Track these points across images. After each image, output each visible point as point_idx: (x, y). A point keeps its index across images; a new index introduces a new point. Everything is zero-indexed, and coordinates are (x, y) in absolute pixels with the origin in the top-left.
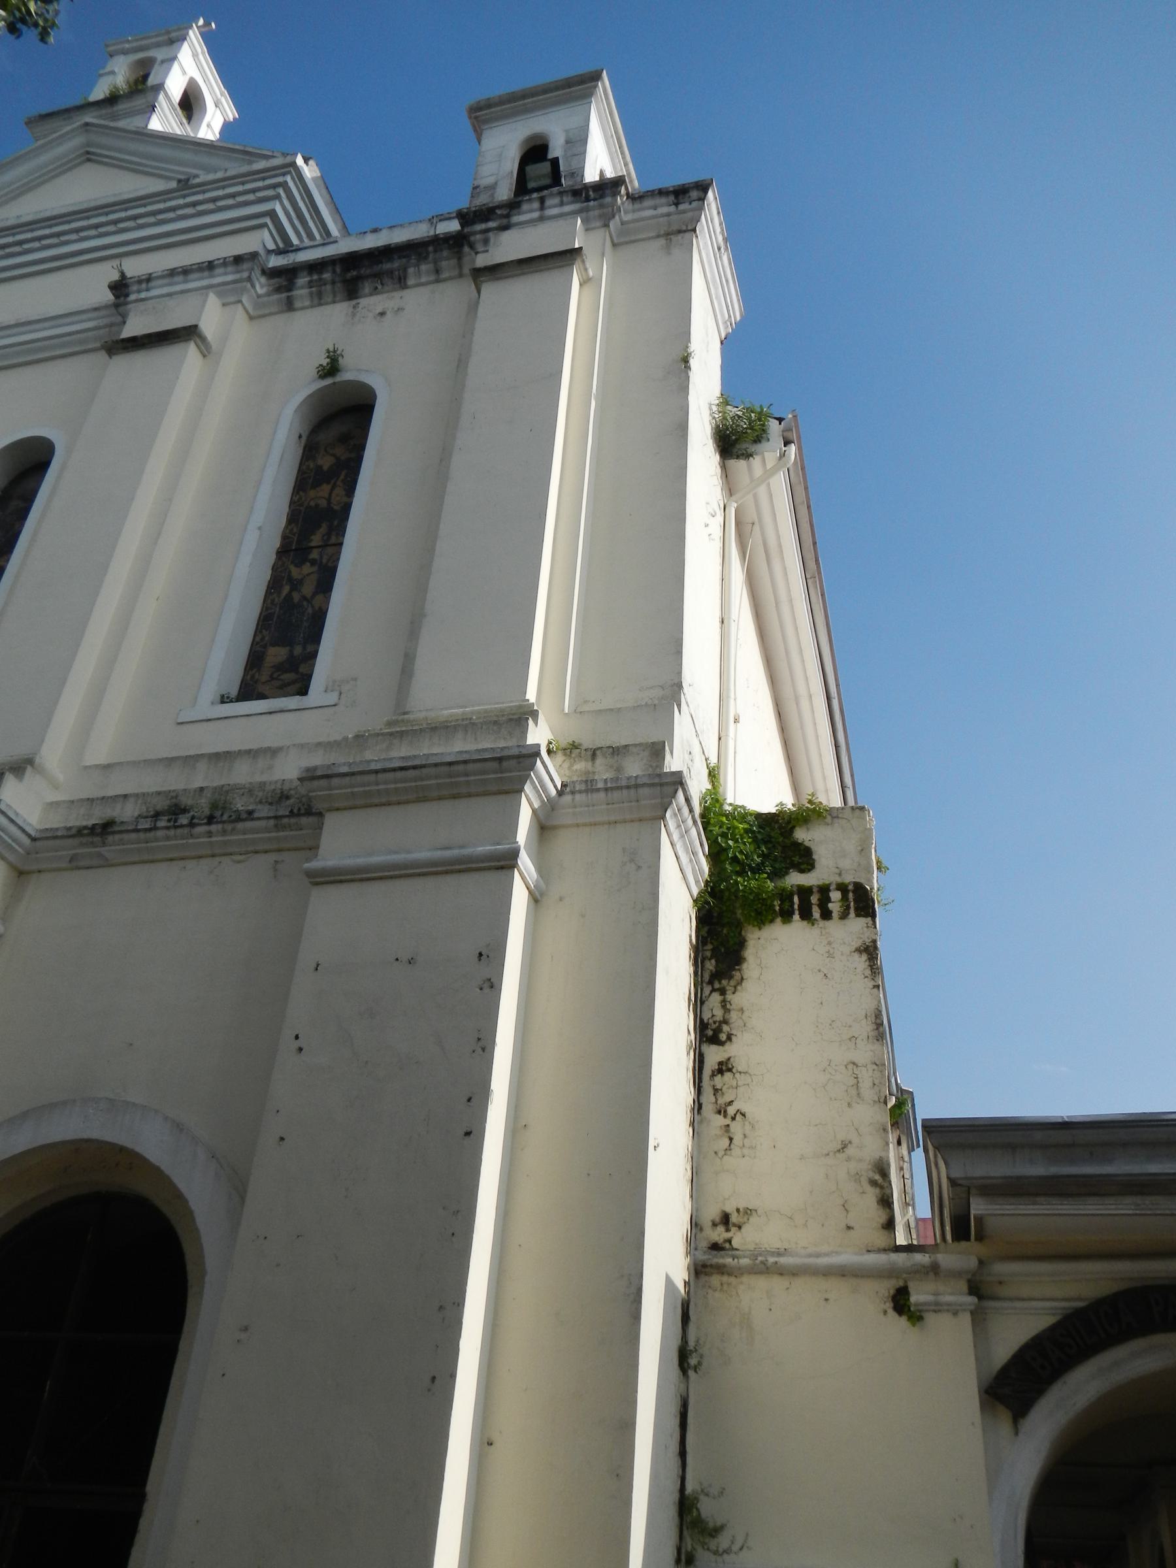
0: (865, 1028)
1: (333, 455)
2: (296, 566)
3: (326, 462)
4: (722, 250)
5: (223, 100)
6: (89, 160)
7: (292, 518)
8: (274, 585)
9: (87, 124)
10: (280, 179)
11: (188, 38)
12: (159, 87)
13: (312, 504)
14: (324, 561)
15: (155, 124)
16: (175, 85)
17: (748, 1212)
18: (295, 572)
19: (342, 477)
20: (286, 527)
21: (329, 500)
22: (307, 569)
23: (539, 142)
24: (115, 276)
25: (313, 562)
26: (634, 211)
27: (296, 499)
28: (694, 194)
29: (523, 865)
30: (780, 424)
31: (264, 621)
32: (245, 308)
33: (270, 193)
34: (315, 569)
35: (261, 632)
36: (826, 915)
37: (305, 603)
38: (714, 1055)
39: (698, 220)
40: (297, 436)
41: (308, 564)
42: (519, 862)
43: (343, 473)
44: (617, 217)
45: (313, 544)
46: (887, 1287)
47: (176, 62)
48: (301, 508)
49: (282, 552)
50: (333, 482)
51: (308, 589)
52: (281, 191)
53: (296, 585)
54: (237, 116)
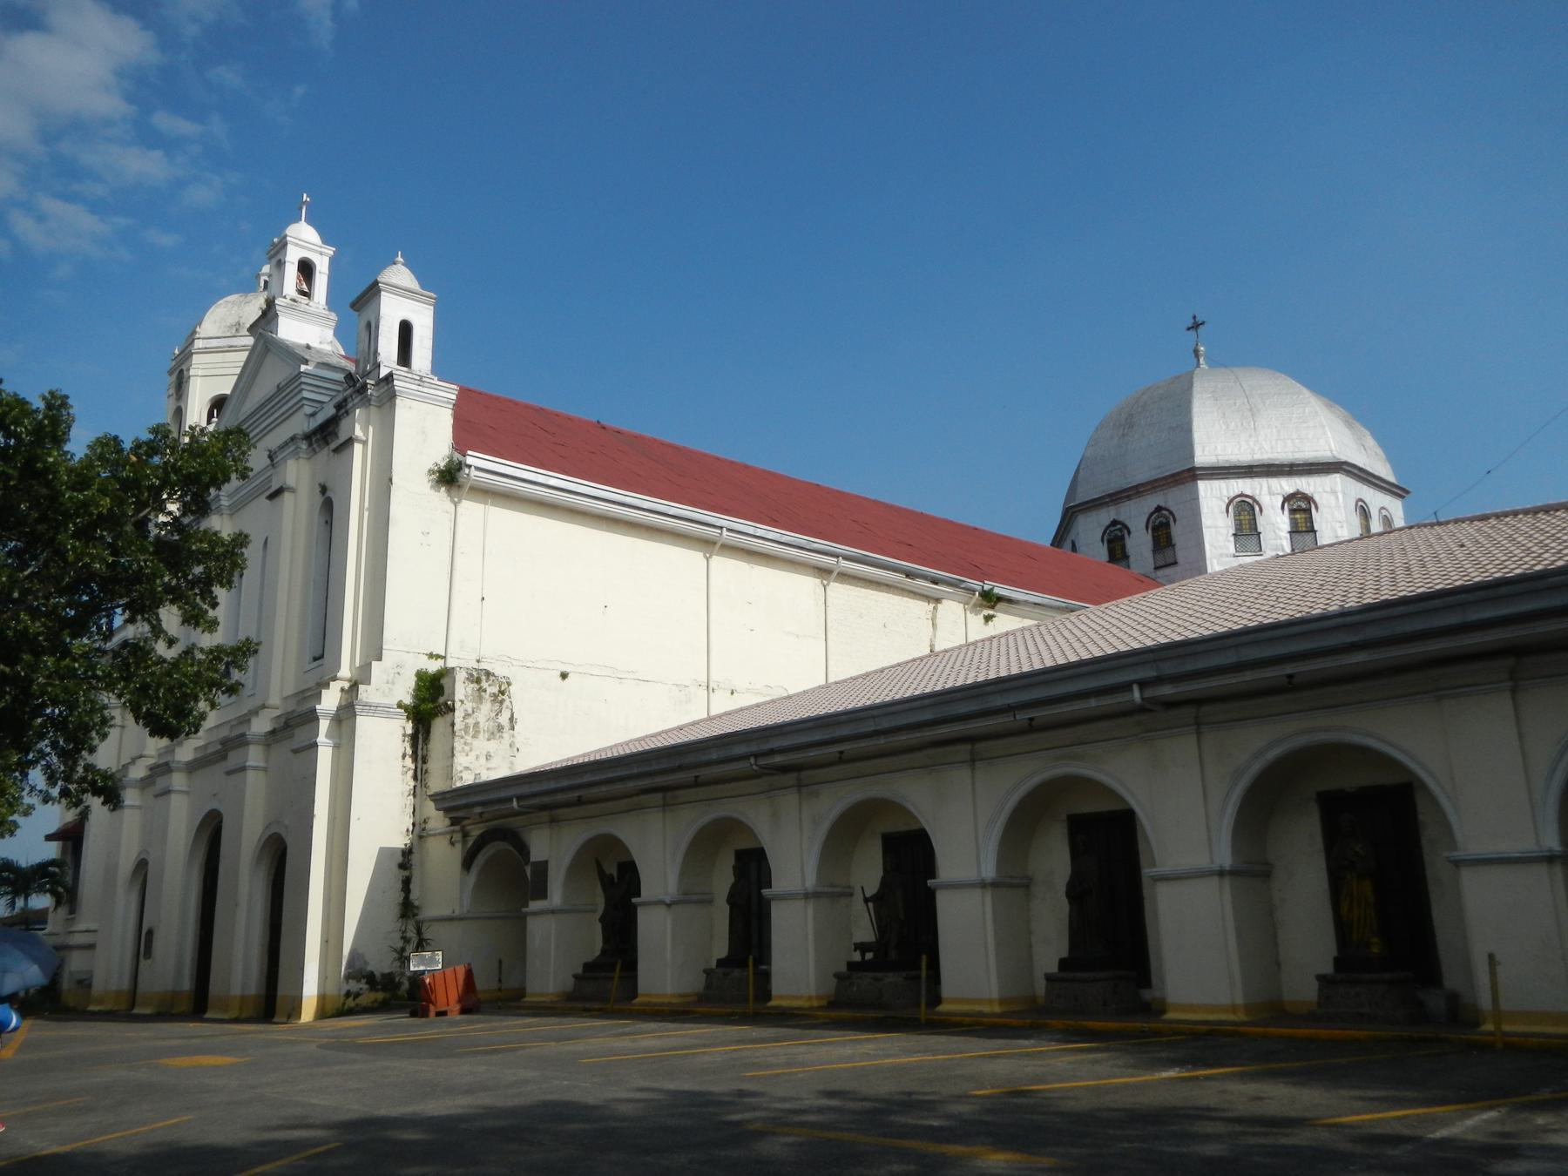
0: (450, 754)
4: (422, 384)
5: (323, 250)
10: (300, 381)
17: (428, 818)
24: (268, 453)
26: (379, 389)
28: (390, 379)
32: (303, 458)
33: (299, 388)
36: (445, 713)
38: (425, 767)
39: (395, 391)
44: (373, 398)
46: (448, 837)
52: (303, 386)
54: (334, 249)
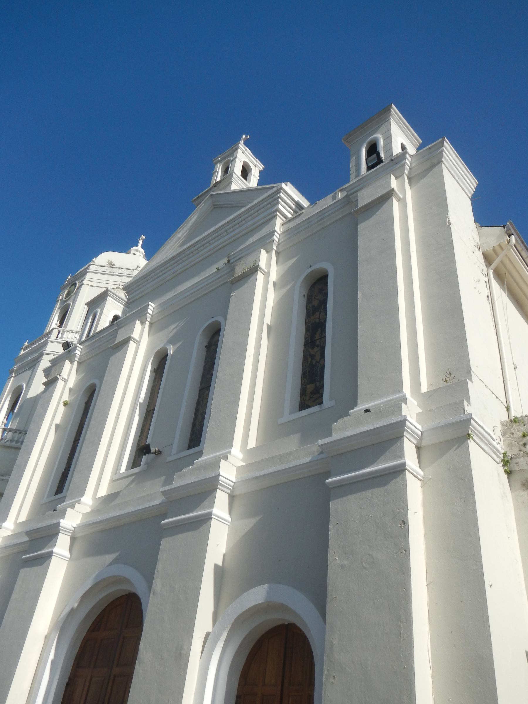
1: (317, 299)
2: (312, 349)
3: (316, 303)
5: (257, 163)
6: (215, 208)
7: (307, 330)
8: (305, 359)
9: (211, 195)
11: (239, 147)
12: (232, 173)
13: (313, 322)
14: (322, 344)
15: (234, 187)
16: (237, 169)
18: (312, 352)
19: (323, 308)
20: (306, 334)
21: (319, 318)
22: (316, 349)
23: (373, 143)
25: (318, 346)
27: (307, 321)
29: (410, 468)
30: (504, 228)
31: (304, 374)
33: (276, 201)
34: (319, 348)
35: (303, 379)
37: (317, 364)
40: (303, 295)
41: (316, 347)
42: (407, 467)
43: (323, 306)
45: (317, 338)
47: (237, 158)
48: (310, 325)
49: (306, 344)
50: (319, 311)
51: (317, 358)
53: (313, 357)
54: (264, 167)
